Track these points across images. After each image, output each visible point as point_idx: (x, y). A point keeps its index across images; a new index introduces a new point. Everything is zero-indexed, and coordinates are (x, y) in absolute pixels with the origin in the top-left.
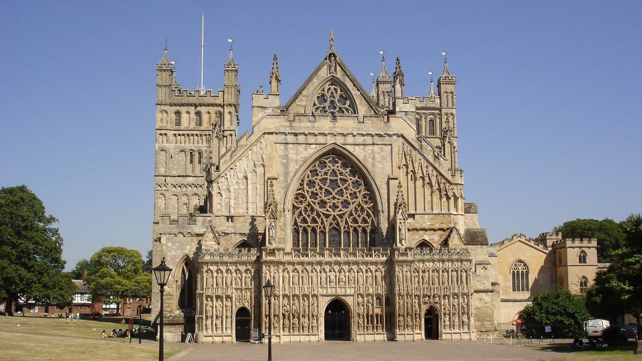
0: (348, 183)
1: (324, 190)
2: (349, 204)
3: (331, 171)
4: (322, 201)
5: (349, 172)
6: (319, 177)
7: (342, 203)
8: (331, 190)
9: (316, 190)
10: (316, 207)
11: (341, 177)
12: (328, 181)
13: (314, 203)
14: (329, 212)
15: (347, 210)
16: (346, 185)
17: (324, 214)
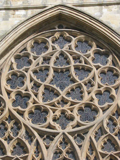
0: (91, 75)
1: (41, 90)
2: (96, 111)
3: (57, 54)
4: (38, 108)
5: (92, 55)
6: (32, 67)
7: (80, 110)
8: (58, 89)
9: (26, 90)
10: (26, 120)
11: (78, 64)
12: (51, 72)
13: (21, 114)
14: (54, 128)
15: (91, 123)
16: (86, 79)
17: (41, 133)
